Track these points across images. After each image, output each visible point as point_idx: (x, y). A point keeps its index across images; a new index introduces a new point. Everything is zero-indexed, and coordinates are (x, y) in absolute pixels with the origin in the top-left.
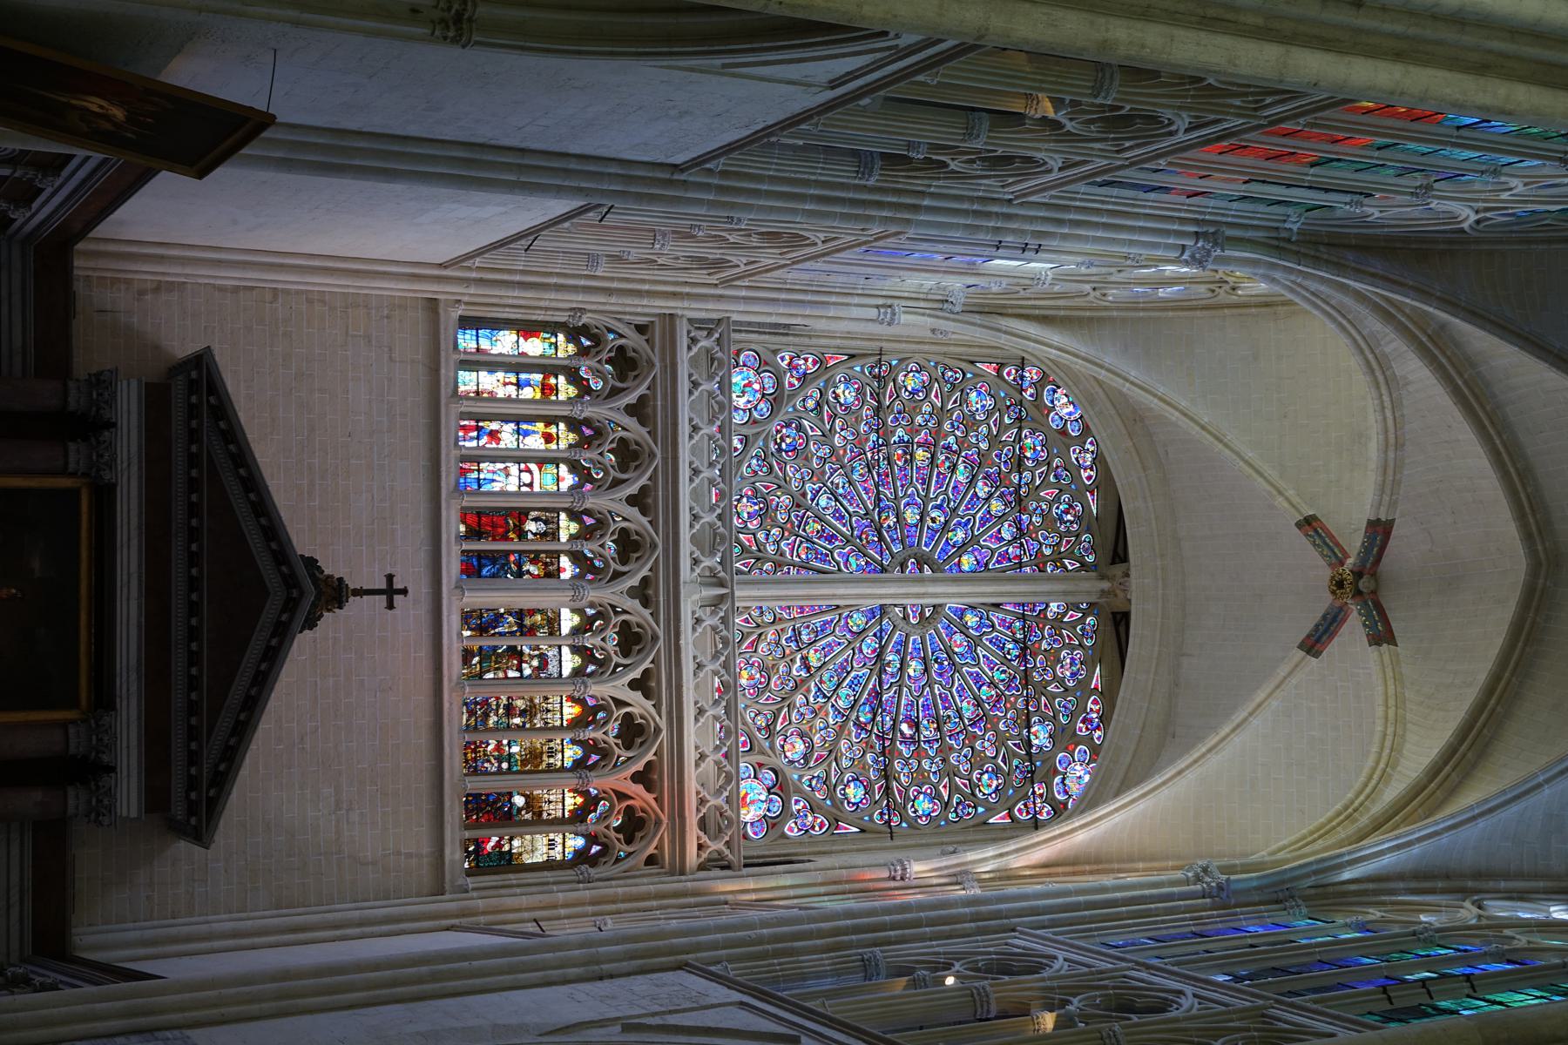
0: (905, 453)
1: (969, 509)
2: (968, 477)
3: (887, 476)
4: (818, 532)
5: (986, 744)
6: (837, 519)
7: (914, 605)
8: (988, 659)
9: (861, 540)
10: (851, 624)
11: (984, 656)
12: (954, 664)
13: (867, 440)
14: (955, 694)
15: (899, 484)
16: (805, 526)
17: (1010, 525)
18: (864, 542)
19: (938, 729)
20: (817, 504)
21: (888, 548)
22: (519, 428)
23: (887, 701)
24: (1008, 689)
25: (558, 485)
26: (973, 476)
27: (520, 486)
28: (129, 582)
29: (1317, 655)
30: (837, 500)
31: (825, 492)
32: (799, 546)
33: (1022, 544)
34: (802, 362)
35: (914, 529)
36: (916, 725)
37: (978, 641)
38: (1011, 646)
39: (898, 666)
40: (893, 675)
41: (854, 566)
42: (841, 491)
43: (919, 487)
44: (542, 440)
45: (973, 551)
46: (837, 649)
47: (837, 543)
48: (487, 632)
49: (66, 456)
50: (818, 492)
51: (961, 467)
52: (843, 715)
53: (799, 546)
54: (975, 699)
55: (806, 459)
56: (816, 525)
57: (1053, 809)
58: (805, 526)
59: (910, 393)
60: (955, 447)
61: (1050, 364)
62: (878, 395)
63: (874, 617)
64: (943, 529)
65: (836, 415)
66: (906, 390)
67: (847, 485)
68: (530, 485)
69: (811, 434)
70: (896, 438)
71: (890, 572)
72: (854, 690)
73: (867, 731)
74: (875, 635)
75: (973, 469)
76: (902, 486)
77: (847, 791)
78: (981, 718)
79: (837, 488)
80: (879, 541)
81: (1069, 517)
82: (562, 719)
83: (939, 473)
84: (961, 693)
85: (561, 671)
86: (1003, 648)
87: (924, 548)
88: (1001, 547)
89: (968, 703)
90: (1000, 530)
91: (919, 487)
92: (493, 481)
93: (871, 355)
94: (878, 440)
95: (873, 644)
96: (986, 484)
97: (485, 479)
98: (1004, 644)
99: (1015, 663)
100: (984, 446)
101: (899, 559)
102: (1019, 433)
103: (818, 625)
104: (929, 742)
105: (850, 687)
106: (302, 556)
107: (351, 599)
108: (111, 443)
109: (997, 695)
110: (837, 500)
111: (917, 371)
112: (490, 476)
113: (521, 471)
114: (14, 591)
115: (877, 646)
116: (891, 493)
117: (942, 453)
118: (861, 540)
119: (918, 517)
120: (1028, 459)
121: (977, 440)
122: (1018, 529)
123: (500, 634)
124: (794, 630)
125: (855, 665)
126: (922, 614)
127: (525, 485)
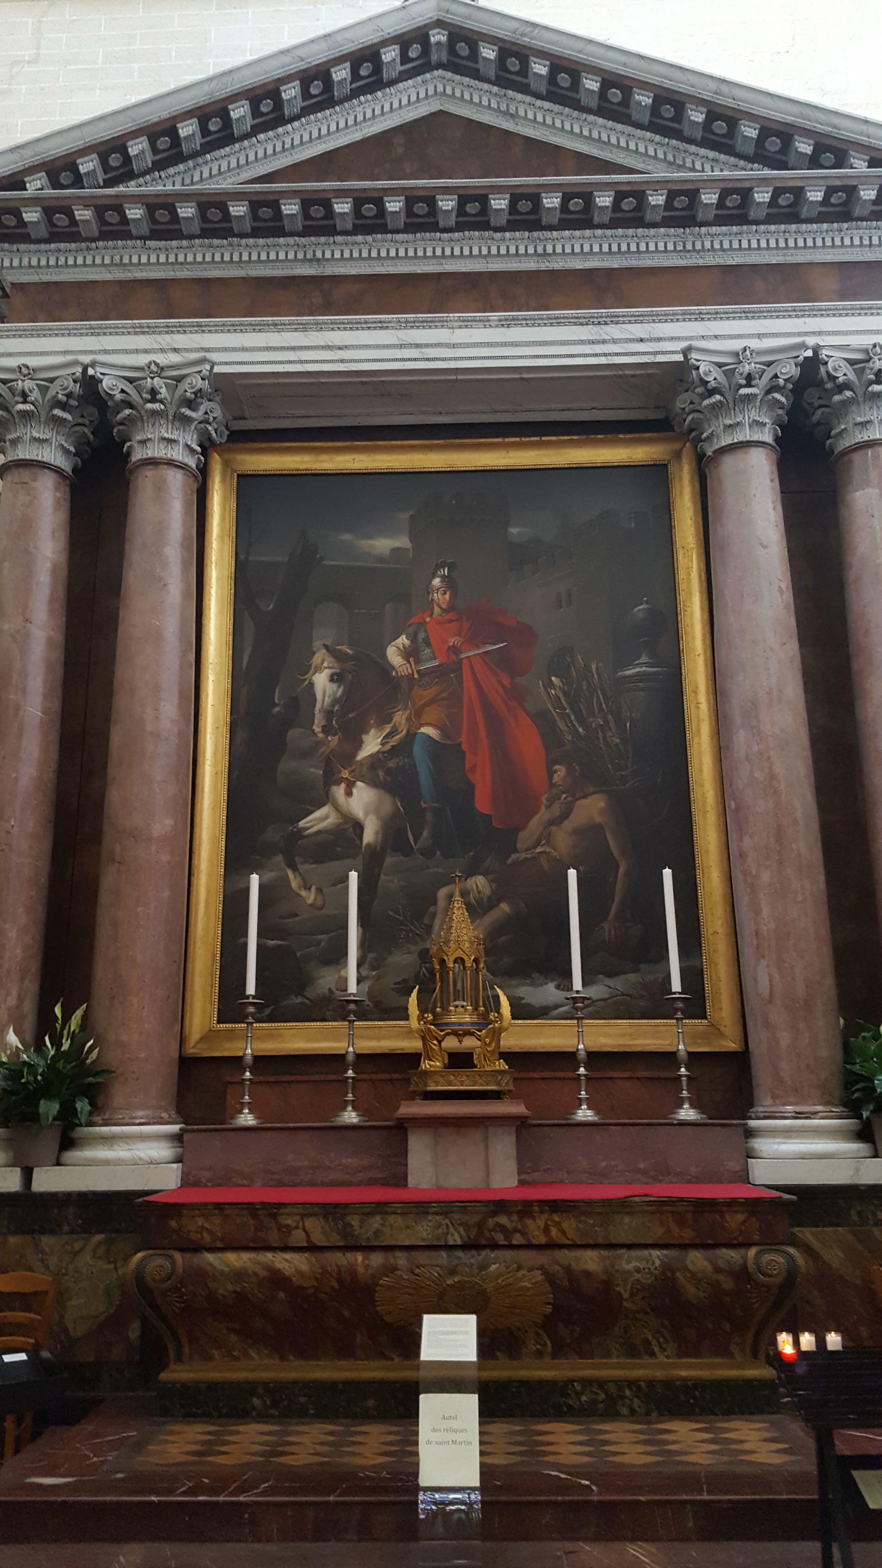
28: (417, 346)
49: (153, 462)
108: (130, 380)
114: (437, 582)
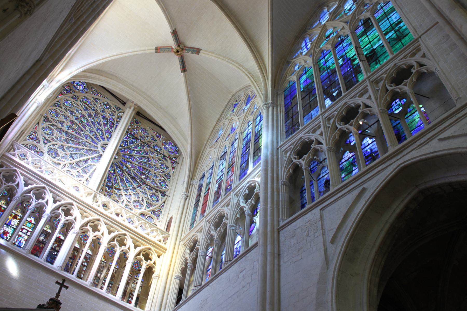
0: (72, 129)
2: (86, 120)
10: (111, 172)
12: (132, 155)
14: (139, 160)
22: (7, 224)
25: (32, 223)
27: (27, 235)
29: (186, 71)
34: (32, 136)
36: (143, 174)
37: (129, 147)
44: (15, 220)
48: (68, 269)
51: (83, 120)
54: (143, 157)
57: (175, 158)
59: (57, 117)
61: (73, 78)
62: (53, 124)
65: (53, 138)
66: (55, 117)
68: (28, 231)
72: (129, 182)
74: (117, 168)
77: (153, 200)
81: (108, 106)
82: (104, 262)
83: (82, 126)
85: (90, 254)
89: (143, 158)
92: (20, 241)
93: (41, 118)
97: (18, 244)
98: (132, 141)
106: (36, 308)
107: (59, 299)
110: (77, 153)
111: (51, 111)
112: (18, 242)
113: (22, 232)
119: (91, 138)
123: (71, 266)
124: (107, 186)
127: (27, 233)
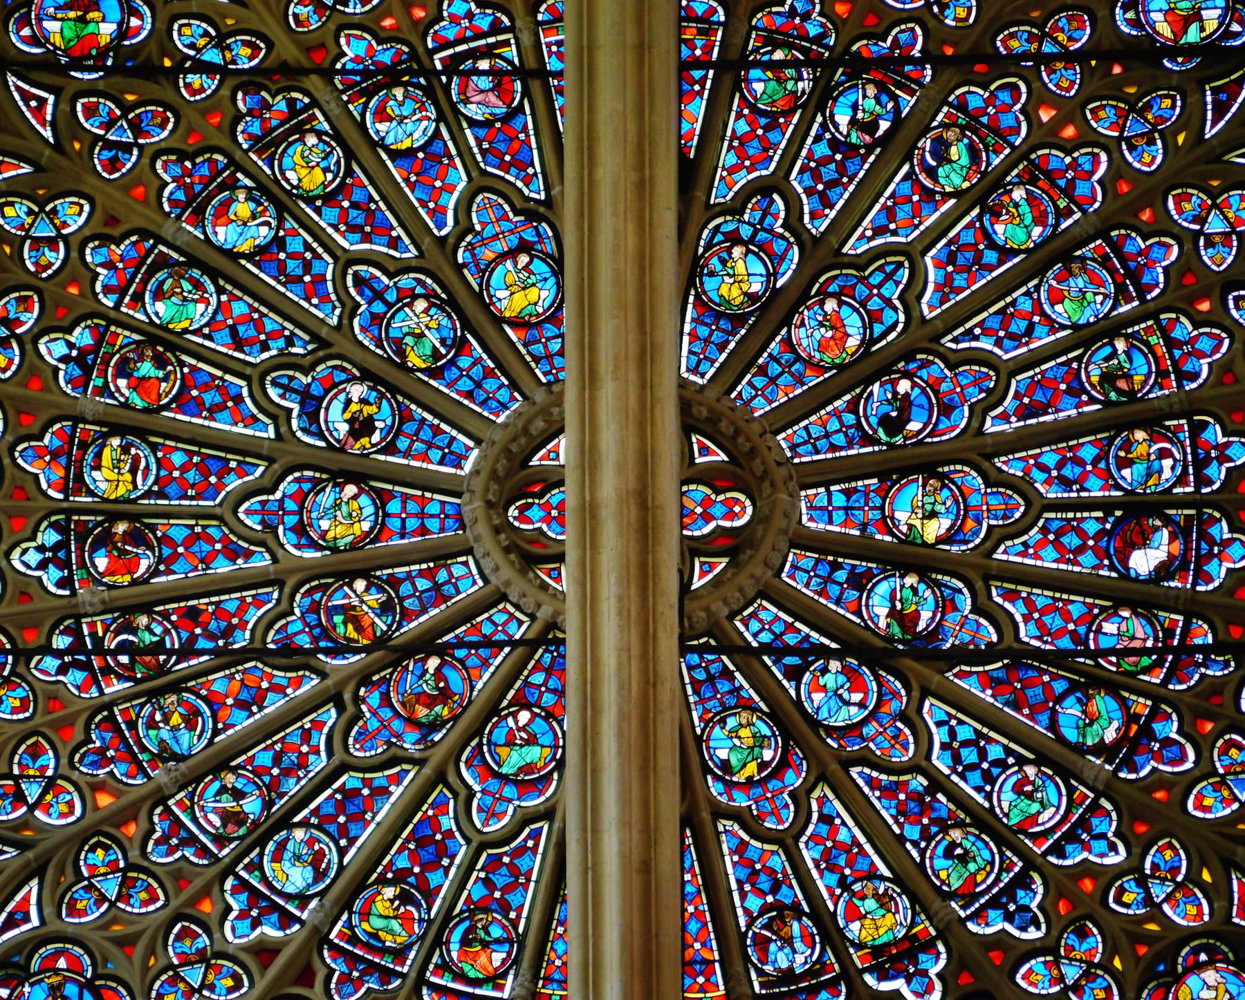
0: (105, 541)
1: (321, 279)
2: (198, 285)
3: (193, 615)
4: (405, 898)
5: (1215, 225)
6: (359, 818)
7: (684, 513)
8: (890, 213)
9: (434, 726)
11: (879, 231)
13: (53, 697)
15: (222, 567)
16: (383, 951)
17: (381, 115)
18: (442, 710)
19: (1153, 422)
20: (302, 899)
21: (468, 614)
23: (1043, 628)
24: (1004, 135)
26: (193, 261)
30: (285, 822)
31: (256, 866)
32: (461, 977)
33: (452, 65)
35: (394, 506)
38: (843, 119)
39: (911, 580)
40: (946, 605)
41: (533, 754)
42: (252, 806)
43: (234, 483)
45: (486, 271)
46: (849, 831)
47: (447, 822)
50: (255, 894)
51: (162, 310)
52: (1095, 808)
53: (461, 977)
54: (1041, 272)
55: (126, 943)
56: (380, 907)
58: (383, 951)
60: (82, 336)
63: (727, 674)
64: (394, 390)
67: (230, 779)
69: (35, 921)
70: (51, 577)
71: (557, 613)
73: (1155, 714)
75: (162, 262)
76: (232, 553)
78: (1117, 247)
79: (236, 818)
80: (443, 651)
83: (182, 401)
84: (1019, 326)
86: (850, 150)
87: (468, 466)
88: (464, 152)
90: (395, 155)
91: (234, 483)
94: (58, 654)
95: (829, 680)
96: (222, 213)
98: (834, 144)
99: (908, 102)
100: (74, 216)
101: (505, 573)
102: (26, 68)
103: (754, 903)
104: (1201, 464)
105: (989, 778)
109: (1028, 179)
115: (834, 665)
116: (258, 604)
117: (104, 390)
118: (434, 726)
119: (351, 490)
120: (123, 31)
121: (52, 243)
122: (390, 86)
125: (902, 757)
126: (714, 478)
